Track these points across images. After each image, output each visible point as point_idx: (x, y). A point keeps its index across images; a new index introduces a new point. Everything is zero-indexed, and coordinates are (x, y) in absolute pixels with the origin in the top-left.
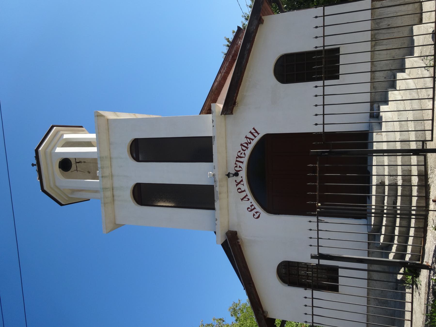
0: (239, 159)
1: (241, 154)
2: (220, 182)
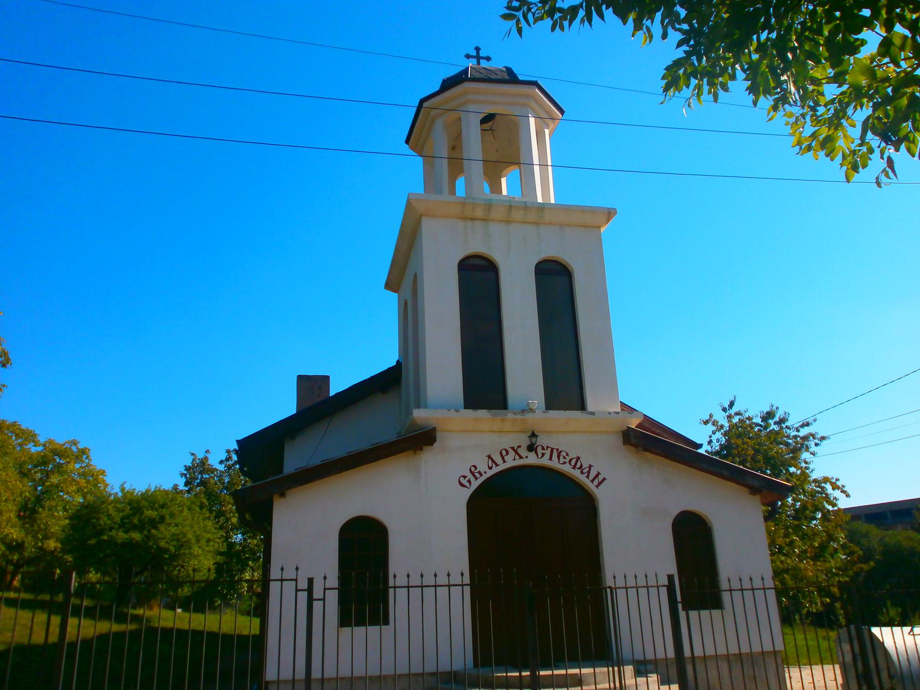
1: (564, 458)
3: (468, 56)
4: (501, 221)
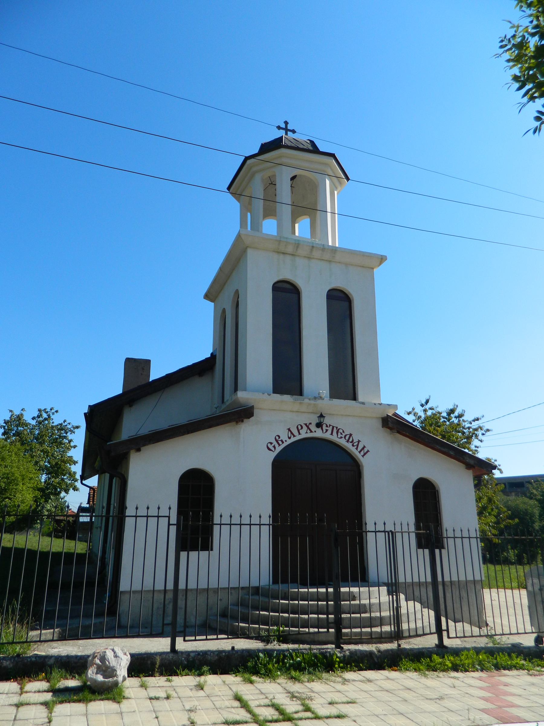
1: (341, 434)
2: (314, 404)
3: (279, 128)
4: (305, 257)
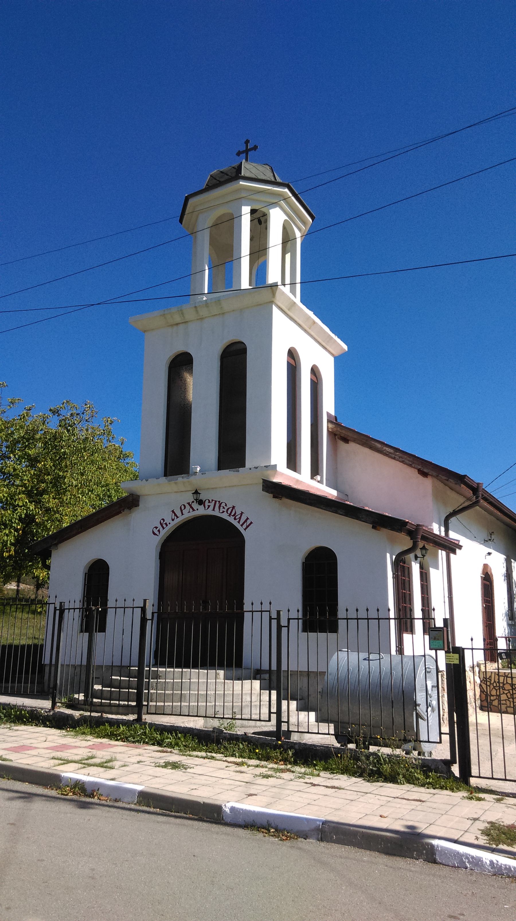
0: (217, 505)
1: (224, 508)
